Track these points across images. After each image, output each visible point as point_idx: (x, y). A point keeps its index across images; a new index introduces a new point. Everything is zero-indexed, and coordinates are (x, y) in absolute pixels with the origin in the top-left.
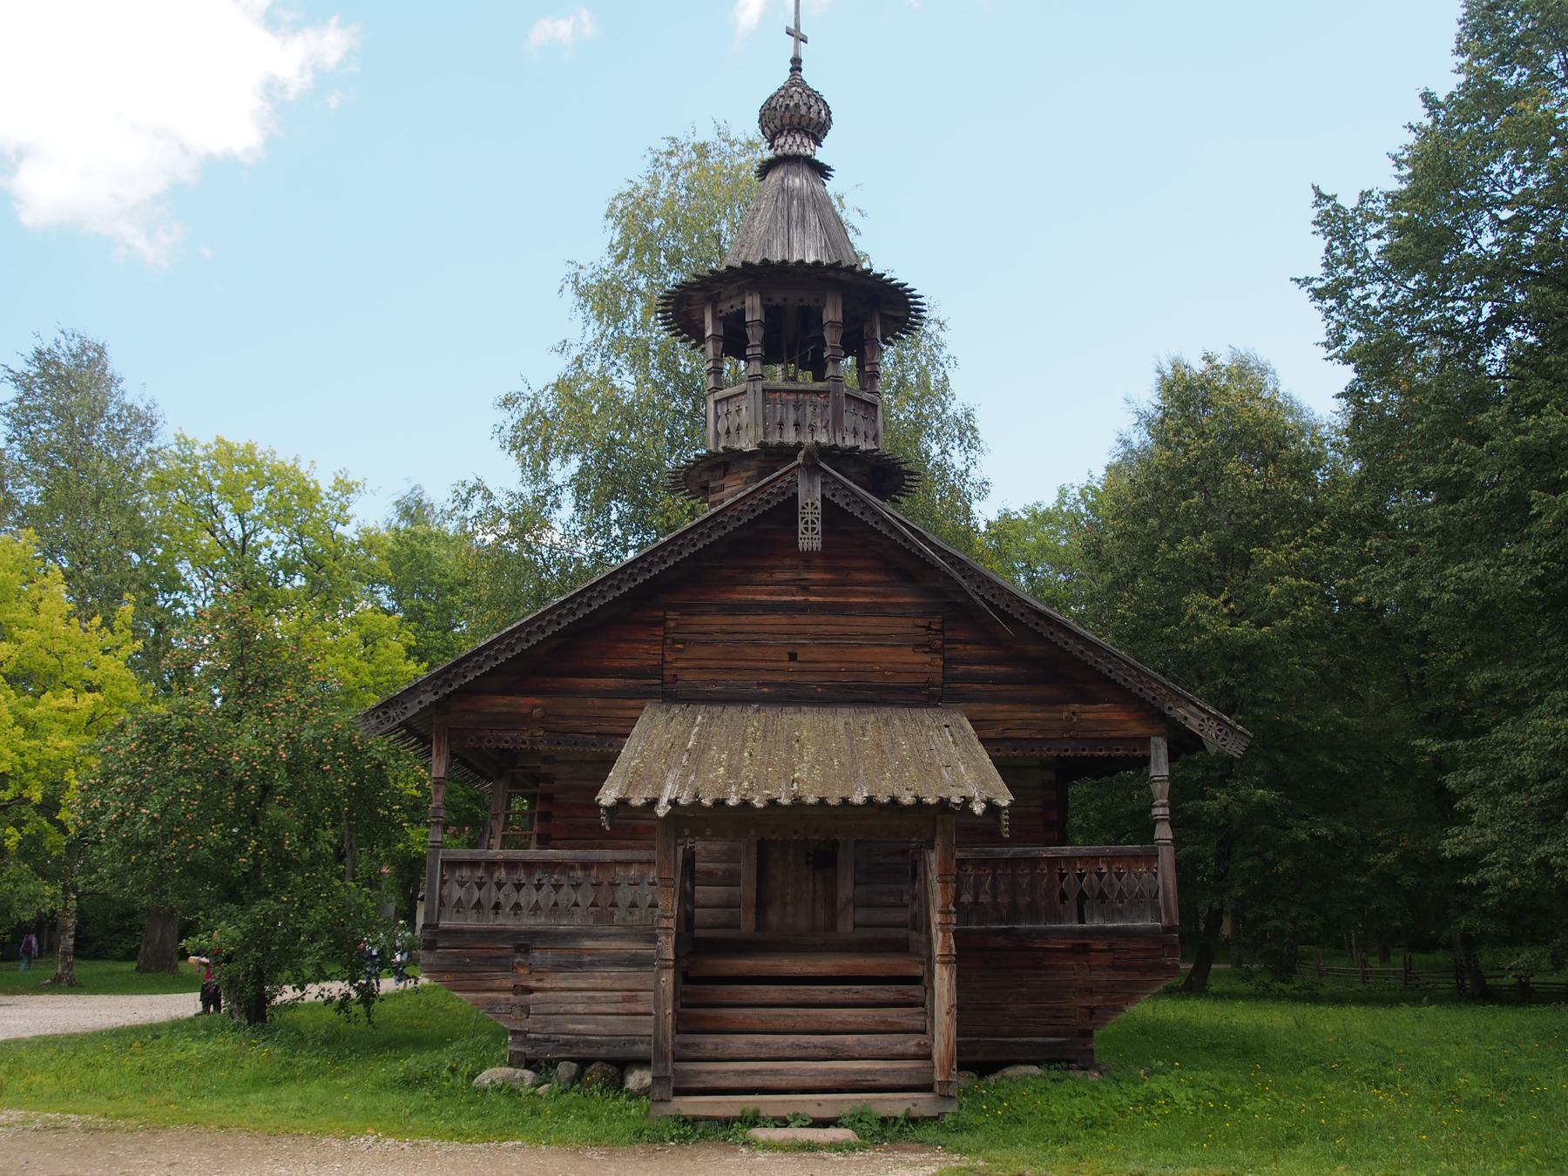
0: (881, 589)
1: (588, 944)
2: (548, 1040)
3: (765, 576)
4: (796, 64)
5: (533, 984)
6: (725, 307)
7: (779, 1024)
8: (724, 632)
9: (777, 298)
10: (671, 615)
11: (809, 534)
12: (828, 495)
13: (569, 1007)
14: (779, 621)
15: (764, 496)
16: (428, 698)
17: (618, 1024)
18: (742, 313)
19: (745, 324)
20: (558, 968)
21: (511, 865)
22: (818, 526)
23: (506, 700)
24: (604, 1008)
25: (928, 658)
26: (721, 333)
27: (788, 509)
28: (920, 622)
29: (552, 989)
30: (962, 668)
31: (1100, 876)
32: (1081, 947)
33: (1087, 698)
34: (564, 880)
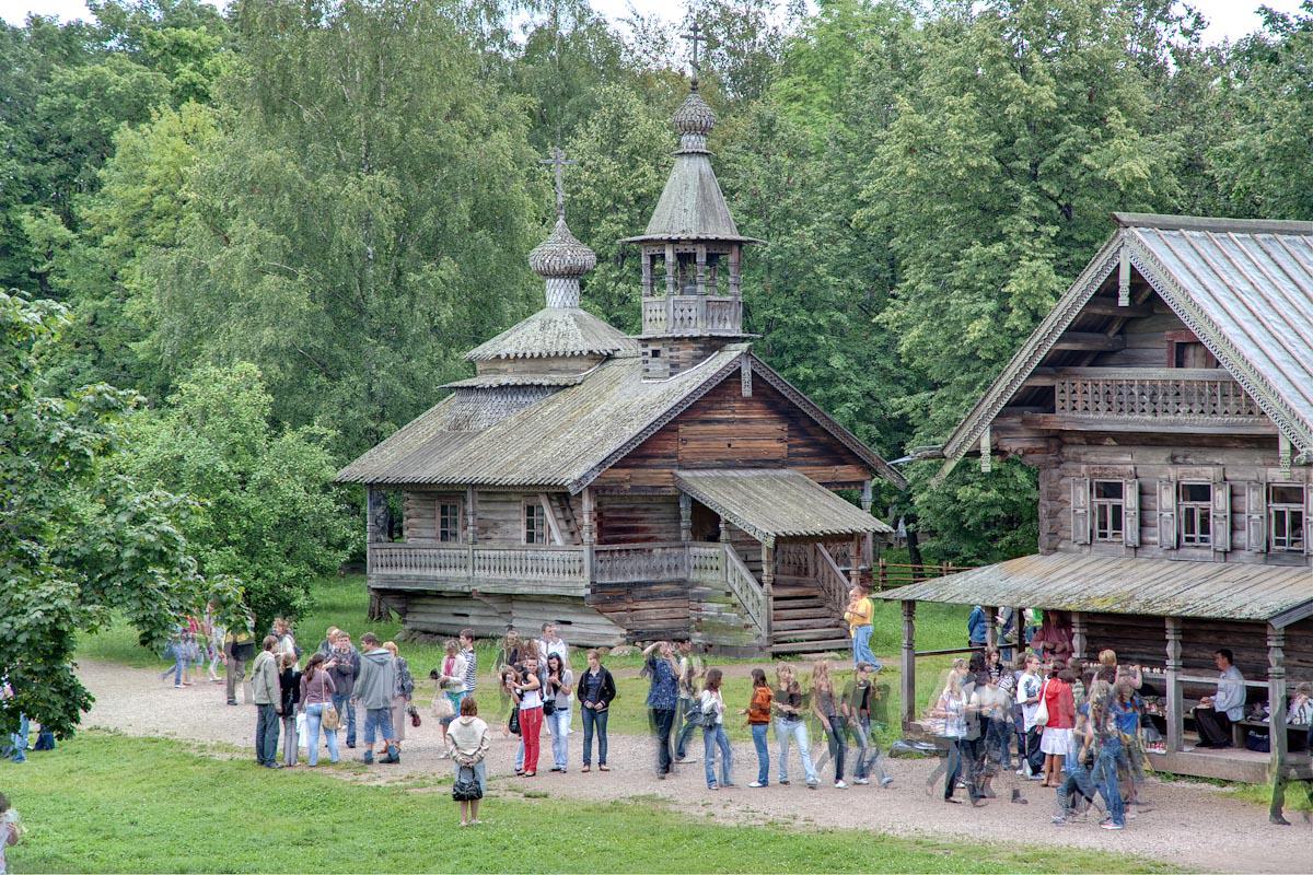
1: (654, 587)
6: (682, 249)
10: (680, 426)
20: (645, 599)
21: (620, 551)
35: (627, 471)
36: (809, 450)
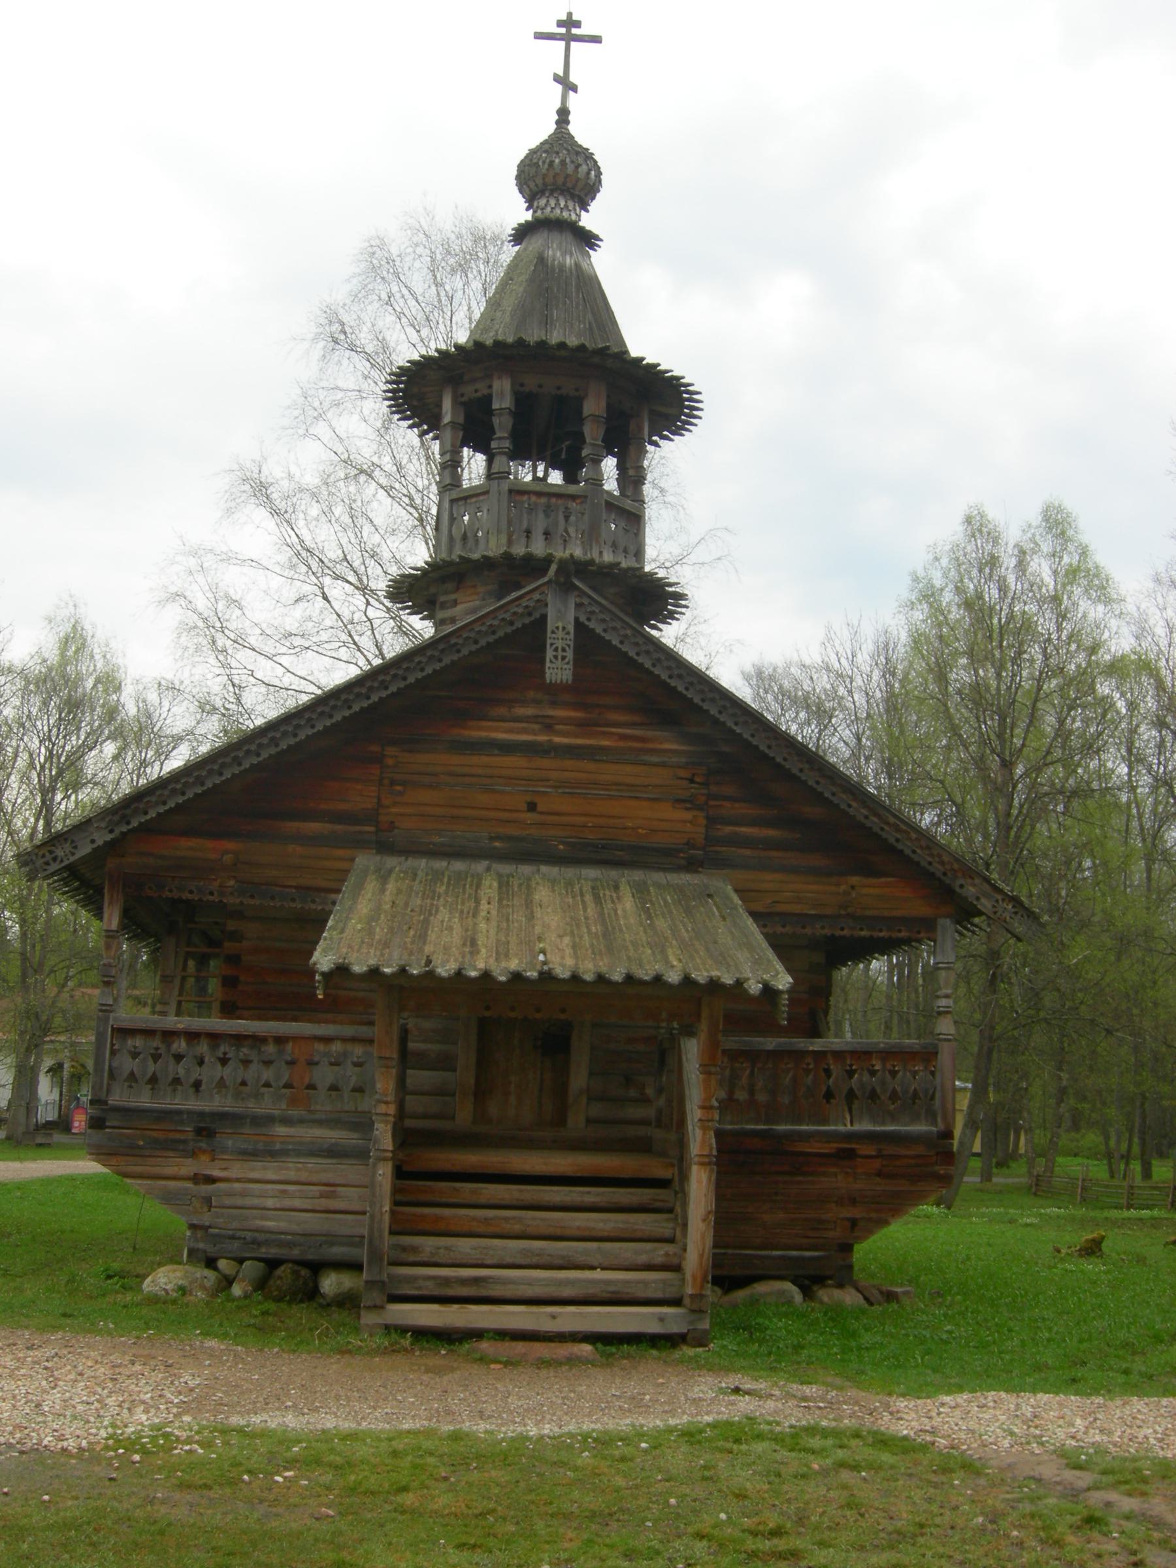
0: (638, 732)
1: (282, 1130)
2: (233, 1237)
3: (502, 711)
4: (563, 115)
5: (216, 1173)
7: (507, 1227)
8: (451, 774)
9: (531, 383)
10: (391, 751)
11: (559, 663)
12: (583, 619)
13: (256, 1202)
14: (515, 763)
15: (507, 616)
16: (102, 838)
17: (313, 1223)
18: (488, 399)
19: (490, 412)
21: (192, 1036)
22: (570, 654)
23: (193, 842)
24: (297, 1203)
25: (688, 815)
26: (461, 420)
27: (533, 634)
28: (682, 773)
29: (238, 1180)
30: (728, 829)
31: (873, 1073)
32: (845, 1153)
33: (869, 871)
34: (254, 1055)
35: (230, 845)
36: (771, 833)
